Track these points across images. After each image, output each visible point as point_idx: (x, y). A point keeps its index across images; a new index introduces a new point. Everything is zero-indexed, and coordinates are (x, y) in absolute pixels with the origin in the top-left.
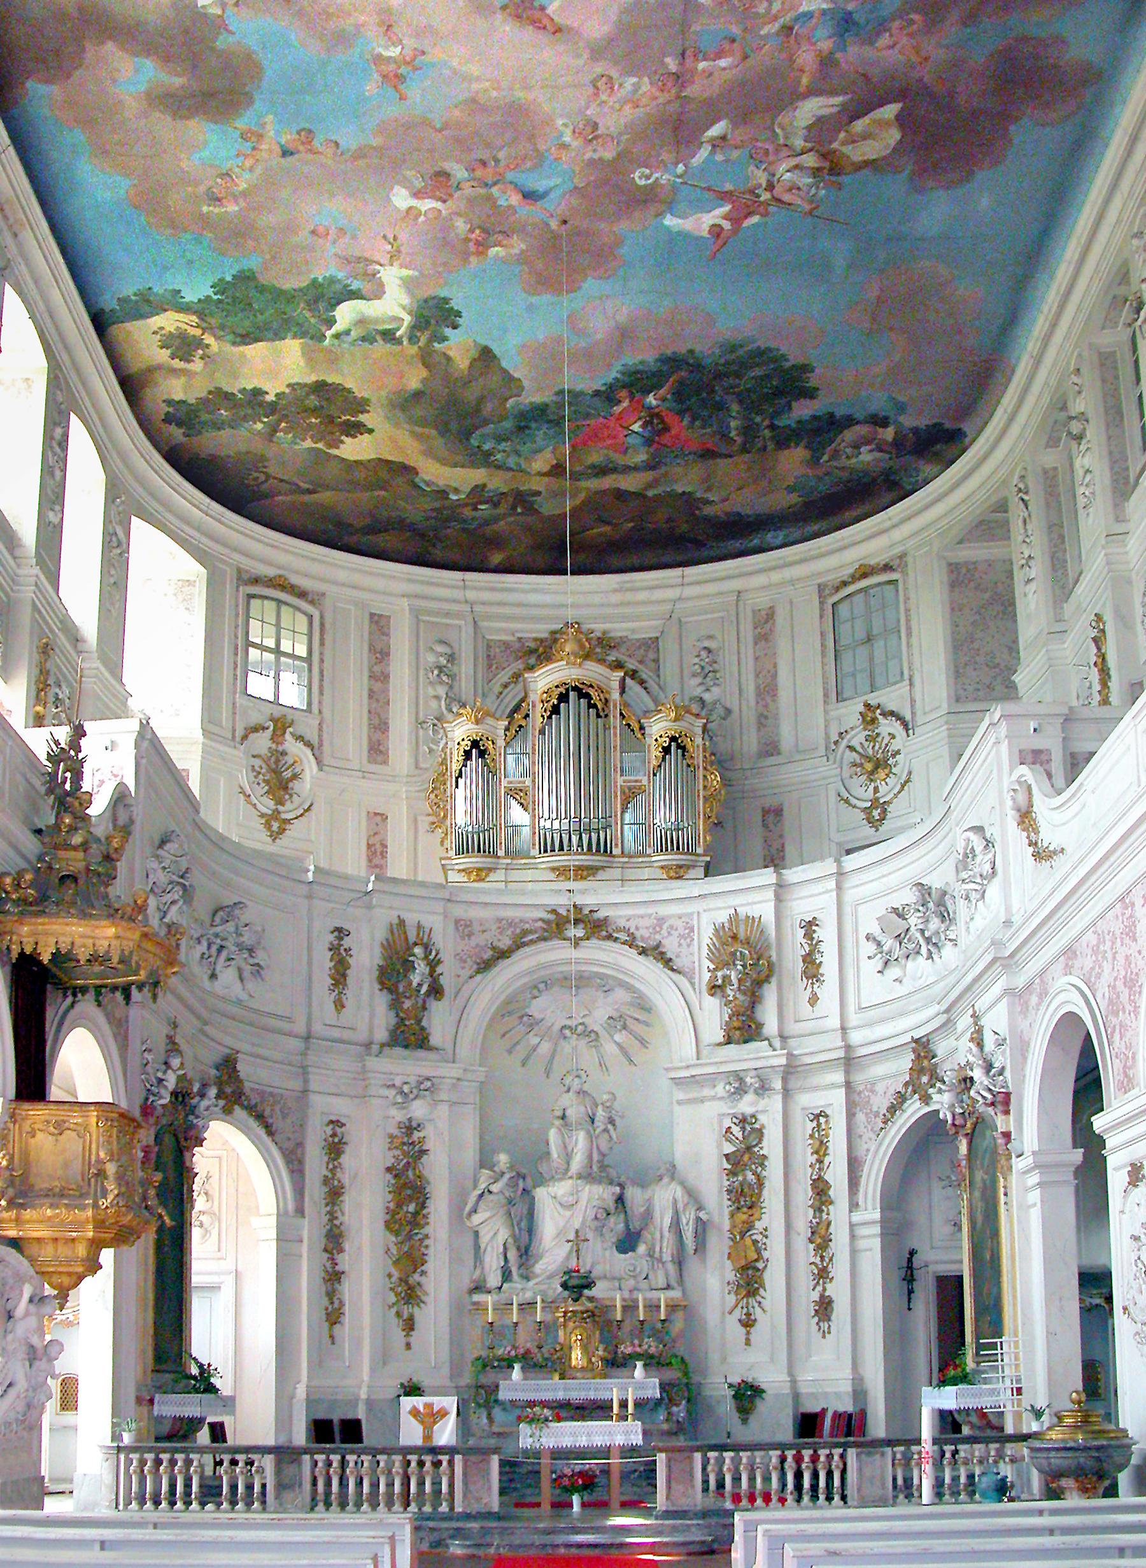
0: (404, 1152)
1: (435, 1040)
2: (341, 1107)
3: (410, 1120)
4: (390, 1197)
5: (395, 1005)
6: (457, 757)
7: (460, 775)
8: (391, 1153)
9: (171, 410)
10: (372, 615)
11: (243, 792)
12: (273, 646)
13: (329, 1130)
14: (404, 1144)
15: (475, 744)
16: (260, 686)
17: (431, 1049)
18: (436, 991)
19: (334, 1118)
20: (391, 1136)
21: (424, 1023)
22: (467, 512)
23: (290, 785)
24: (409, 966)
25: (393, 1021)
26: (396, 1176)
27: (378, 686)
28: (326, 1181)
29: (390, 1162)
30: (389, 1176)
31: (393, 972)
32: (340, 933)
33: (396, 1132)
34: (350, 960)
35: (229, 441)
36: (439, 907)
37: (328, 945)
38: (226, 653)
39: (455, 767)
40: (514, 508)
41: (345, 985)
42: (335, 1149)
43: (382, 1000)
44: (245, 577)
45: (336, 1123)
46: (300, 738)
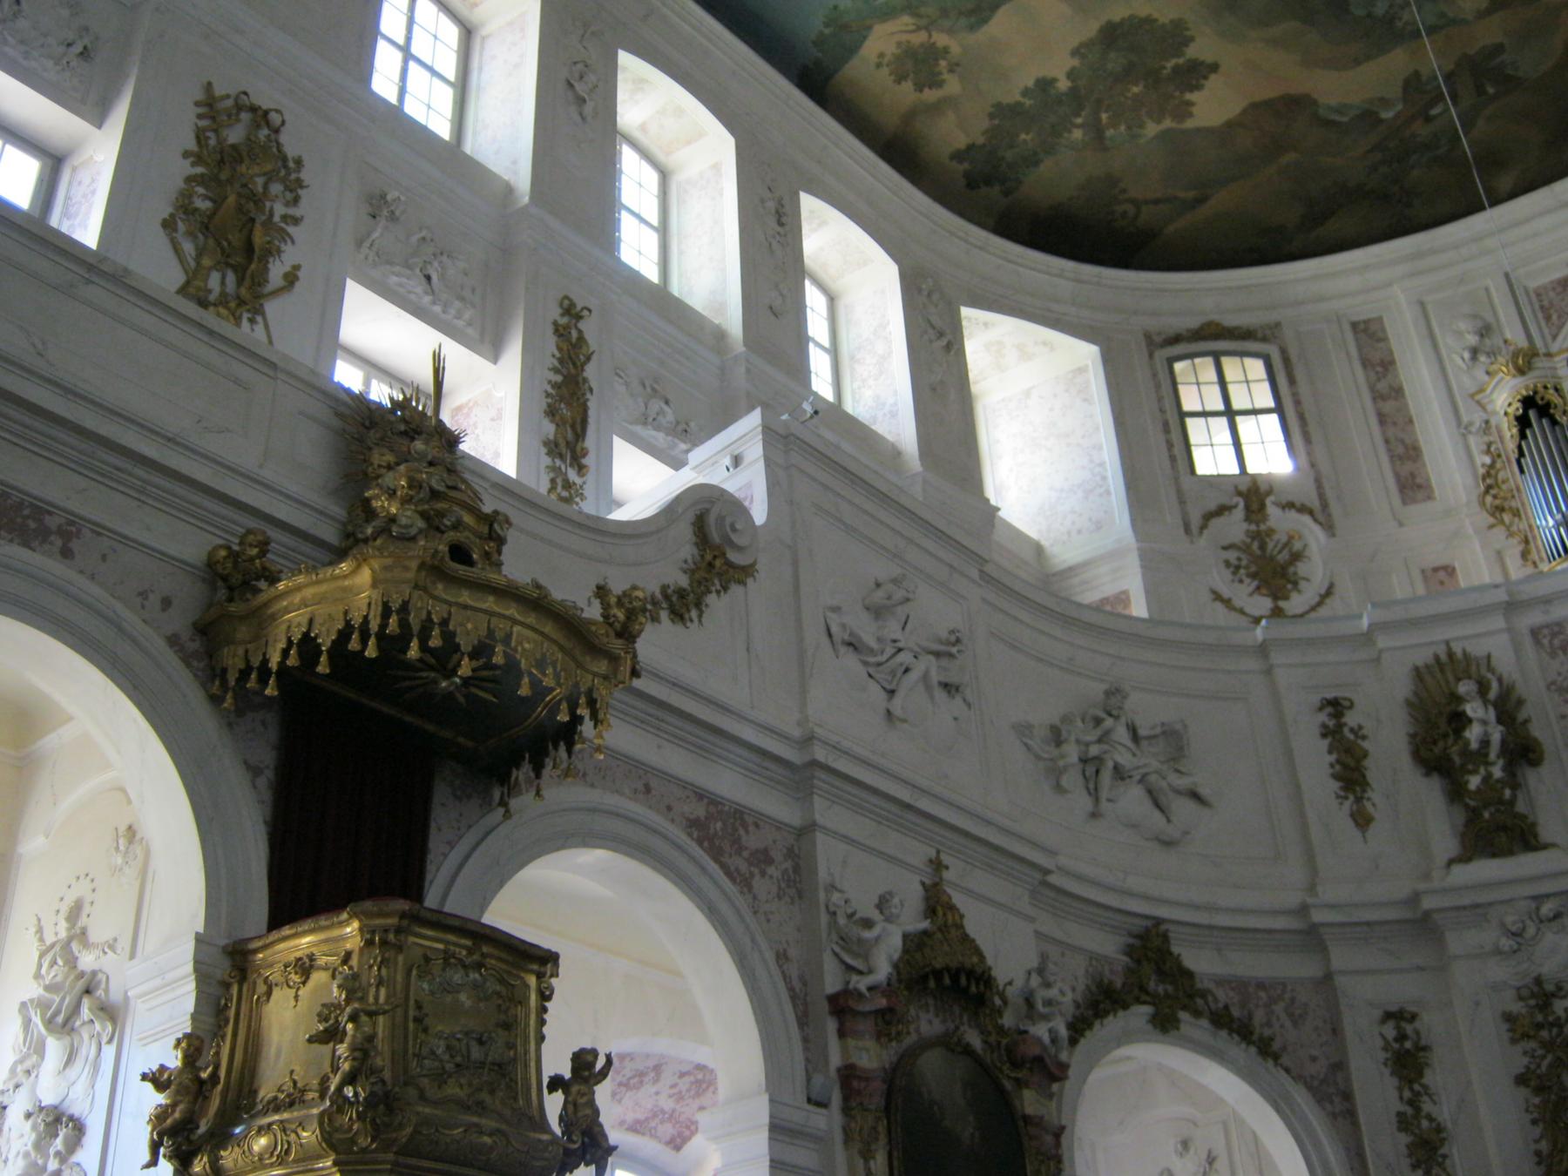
0: (1544, 1045)
1: (1546, 833)
2: (1402, 990)
3: (1538, 981)
4: (1538, 1130)
5: (1456, 793)
6: (1510, 432)
7: (1521, 454)
8: (1519, 1048)
9: (966, 165)
10: (1354, 325)
11: (1217, 596)
12: (1221, 407)
13: (1390, 1031)
14: (1539, 1026)
15: (1528, 402)
16: (1212, 456)
17: (1545, 847)
18: (1523, 751)
19: (1393, 1008)
20: (1509, 1018)
21: (1521, 807)
22: (1422, 131)
23: (1291, 570)
24: (1459, 721)
25: (1460, 816)
26: (1539, 1090)
27: (1388, 407)
28: (1404, 1123)
29: (1520, 1063)
30: (1523, 1092)
31: (1437, 739)
32: (1336, 706)
33: (1517, 1007)
34: (1365, 744)
35: (1061, 172)
36: (1499, 622)
37: (1317, 731)
38: (1149, 432)
39: (1511, 446)
40: (1480, 90)
41: (1364, 784)
42: (1408, 1061)
43: (1431, 792)
44: (1158, 339)
45: (1398, 1016)
46: (1290, 505)
